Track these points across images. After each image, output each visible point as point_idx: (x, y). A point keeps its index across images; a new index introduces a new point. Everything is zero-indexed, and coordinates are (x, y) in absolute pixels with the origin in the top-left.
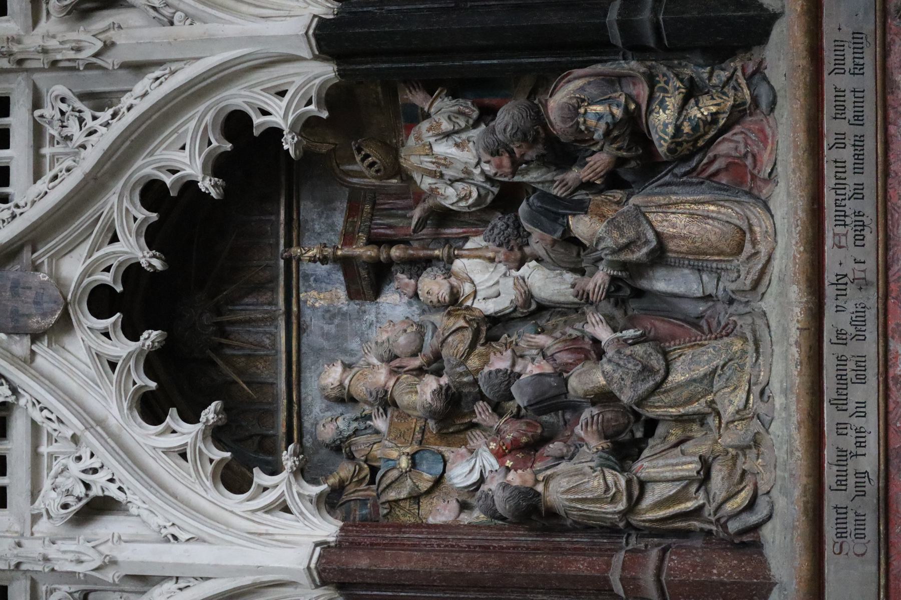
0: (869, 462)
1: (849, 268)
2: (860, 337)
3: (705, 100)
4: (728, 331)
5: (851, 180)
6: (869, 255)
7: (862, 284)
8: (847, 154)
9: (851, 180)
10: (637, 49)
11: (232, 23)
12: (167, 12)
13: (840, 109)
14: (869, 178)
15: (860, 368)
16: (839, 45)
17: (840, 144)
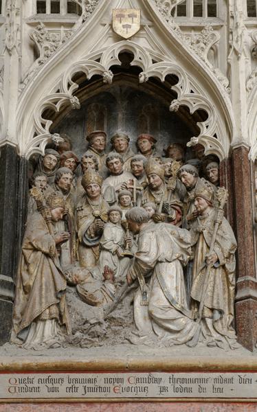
11: (17, 108)
12: (26, 81)
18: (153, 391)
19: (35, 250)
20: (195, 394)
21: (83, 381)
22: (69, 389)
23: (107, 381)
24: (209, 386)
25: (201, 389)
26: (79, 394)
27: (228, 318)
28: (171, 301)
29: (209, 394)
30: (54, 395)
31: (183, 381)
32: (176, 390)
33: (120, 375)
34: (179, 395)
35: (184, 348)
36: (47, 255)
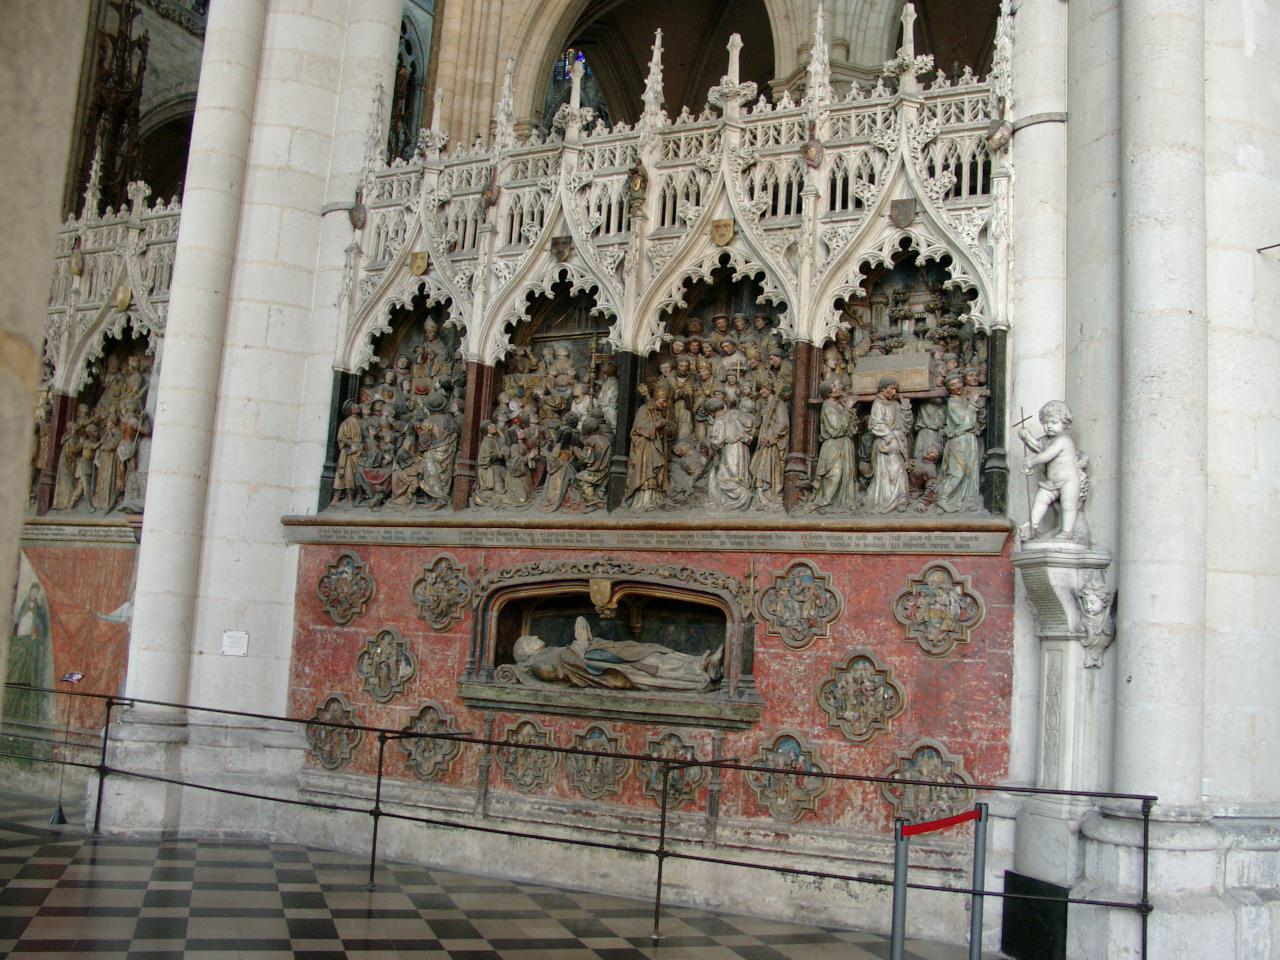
0: (486, 542)
1: (536, 537)
2: (518, 540)
3: (591, 489)
4: (527, 498)
5: (561, 538)
6: (540, 544)
7: (532, 541)
8: (567, 537)
9: (561, 538)
10: (612, 463)
13: (580, 535)
14: (562, 544)
15: (511, 540)
16: (598, 535)
17: (571, 535)
18: (716, 544)
19: (640, 435)
20: (746, 547)
21: (666, 536)
22: (658, 542)
23: (682, 536)
24: (755, 540)
25: (749, 543)
26: (665, 545)
27: (779, 487)
28: (732, 475)
29: (755, 547)
30: (648, 546)
31: (735, 537)
32: (732, 544)
33: (691, 532)
34: (734, 547)
35: (736, 513)
36: (648, 439)
